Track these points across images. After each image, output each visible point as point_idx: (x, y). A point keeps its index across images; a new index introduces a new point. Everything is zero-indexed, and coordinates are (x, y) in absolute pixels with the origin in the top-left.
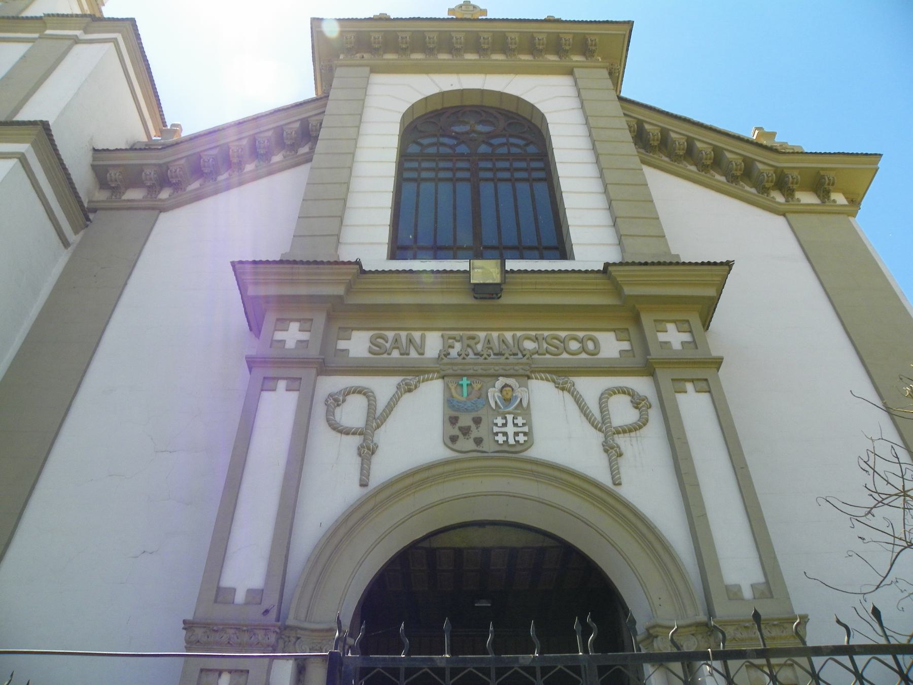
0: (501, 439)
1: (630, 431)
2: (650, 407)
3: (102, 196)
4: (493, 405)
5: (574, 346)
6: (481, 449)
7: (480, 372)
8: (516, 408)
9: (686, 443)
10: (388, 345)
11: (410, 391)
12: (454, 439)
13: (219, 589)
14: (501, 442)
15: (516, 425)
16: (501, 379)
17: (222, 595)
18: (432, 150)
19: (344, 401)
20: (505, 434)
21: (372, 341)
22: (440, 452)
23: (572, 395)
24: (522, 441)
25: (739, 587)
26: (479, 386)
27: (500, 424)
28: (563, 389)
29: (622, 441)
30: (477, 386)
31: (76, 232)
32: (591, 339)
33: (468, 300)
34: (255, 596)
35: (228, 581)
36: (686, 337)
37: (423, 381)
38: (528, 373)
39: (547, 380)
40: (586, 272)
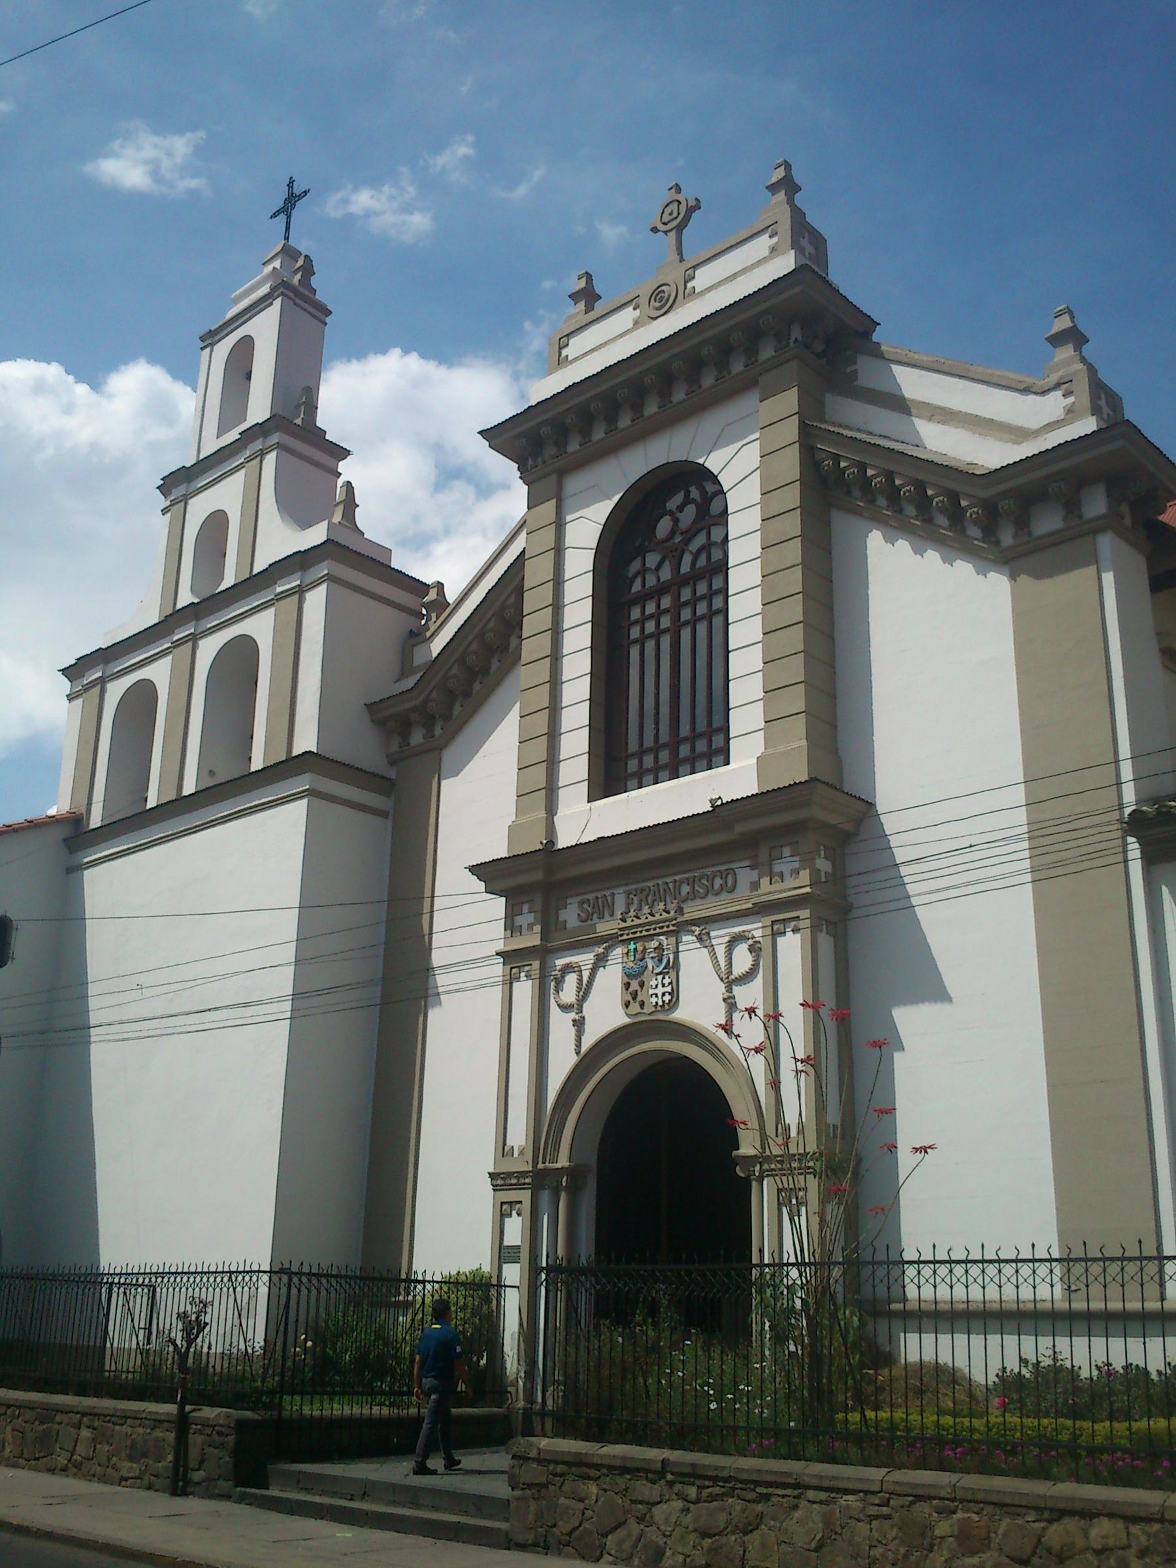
0: (654, 1000)
5: (718, 882)
6: (643, 1011)
7: (644, 933)
8: (664, 969)
10: (590, 909)
15: (663, 985)
16: (655, 937)
19: (563, 977)
20: (657, 995)
21: (582, 903)
22: (619, 1019)
26: (641, 948)
27: (654, 987)
29: (736, 990)
31: (388, 796)
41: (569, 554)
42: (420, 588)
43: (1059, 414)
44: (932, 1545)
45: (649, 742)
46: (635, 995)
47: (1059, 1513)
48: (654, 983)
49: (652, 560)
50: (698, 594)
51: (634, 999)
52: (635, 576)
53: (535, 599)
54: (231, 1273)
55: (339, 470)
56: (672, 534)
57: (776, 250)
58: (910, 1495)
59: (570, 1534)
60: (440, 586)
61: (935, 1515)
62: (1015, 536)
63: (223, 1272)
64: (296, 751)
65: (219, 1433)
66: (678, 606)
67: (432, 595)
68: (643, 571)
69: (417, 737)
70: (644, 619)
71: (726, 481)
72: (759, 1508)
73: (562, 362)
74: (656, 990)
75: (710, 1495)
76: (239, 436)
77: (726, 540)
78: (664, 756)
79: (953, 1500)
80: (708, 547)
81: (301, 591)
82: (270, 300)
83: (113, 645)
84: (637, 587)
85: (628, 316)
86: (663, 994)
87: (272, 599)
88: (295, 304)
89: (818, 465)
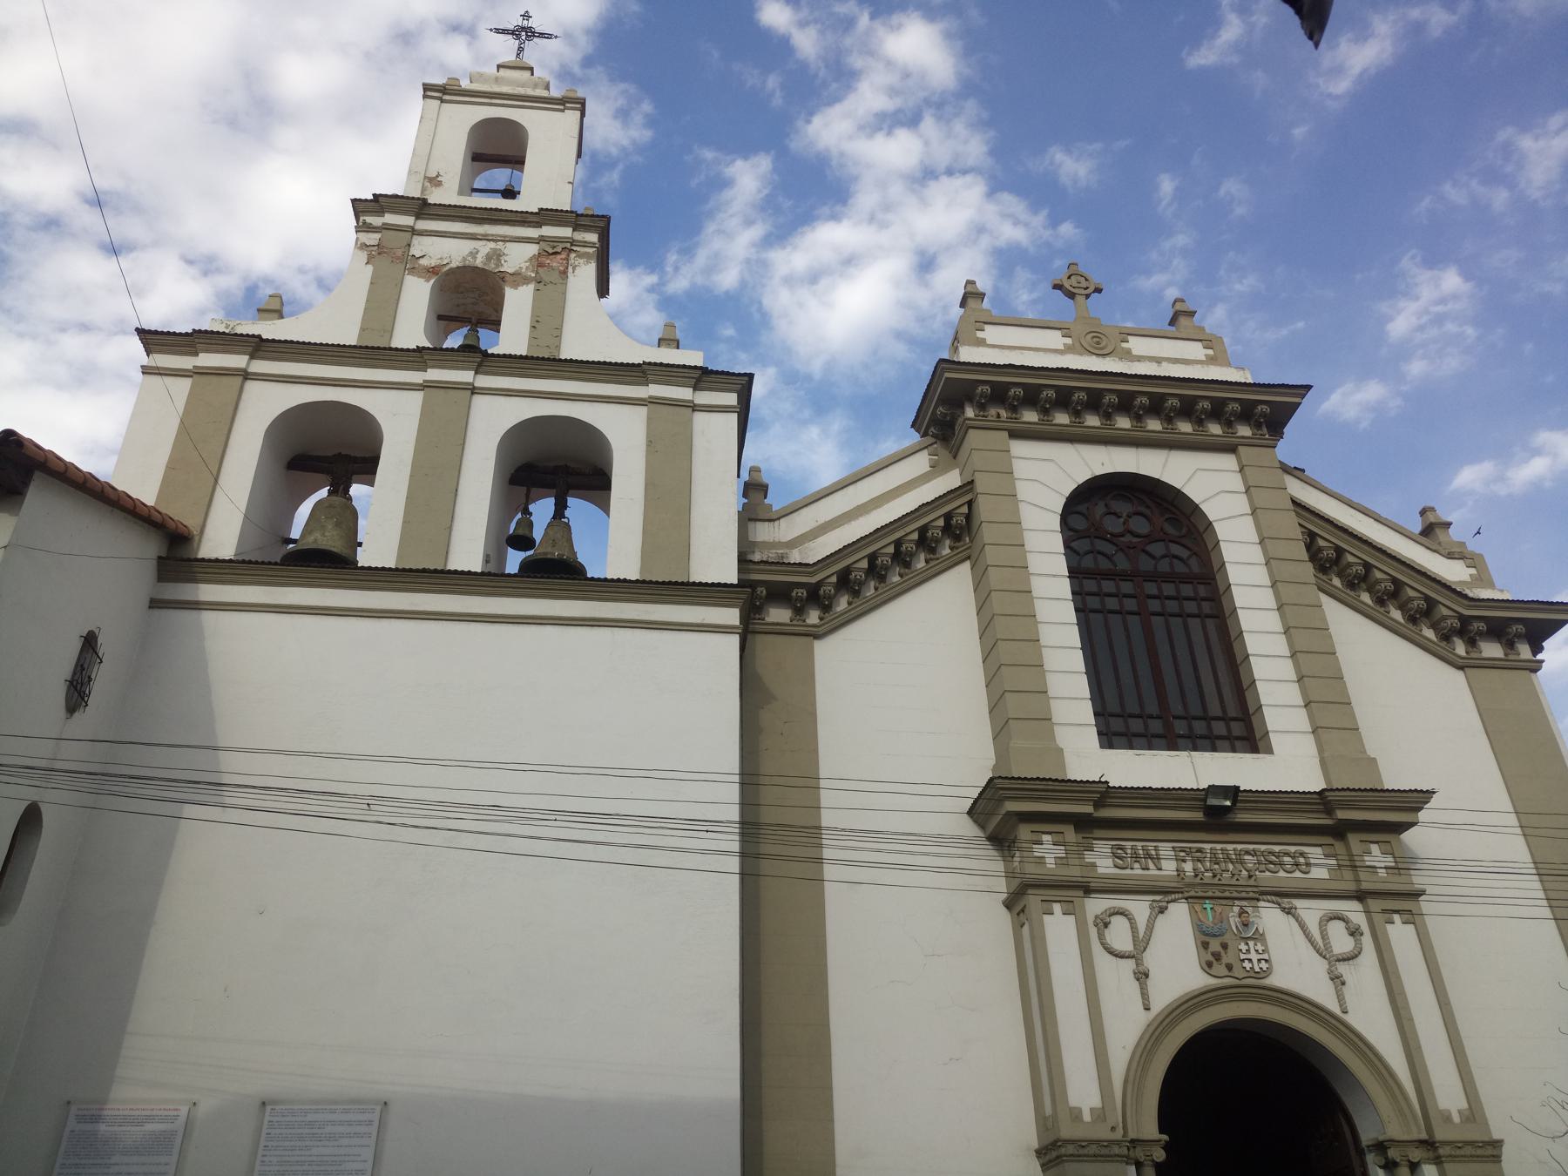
2: (1362, 934)
4: (1235, 931)
7: (1218, 894)
9: (1399, 977)
11: (1162, 912)
12: (1208, 966)
13: (1071, 1109)
14: (1248, 969)
15: (1257, 951)
16: (1237, 902)
17: (1076, 1114)
18: (1088, 562)
19: (1110, 923)
20: (1250, 960)
23: (1297, 920)
24: (1265, 969)
25: (1449, 1111)
26: (1220, 910)
27: (1244, 951)
28: (1288, 913)
29: (1342, 968)
30: (1219, 909)
32: (1302, 854)
34: (1100, 1115)
35: (1074, 1101)
36: (1389, 861)
38: (1257, 896)
39: (1273, 902)
40: (1304, 793)
46: (1217, 956)
57: (1216, 360)
69: (778, 615)
71: (1211, 510)
73: (982, 343)
81: (695, 408)
82: (562, 107)
83: (286, 341)
85: (1055, 339)
86: (1259, 960)
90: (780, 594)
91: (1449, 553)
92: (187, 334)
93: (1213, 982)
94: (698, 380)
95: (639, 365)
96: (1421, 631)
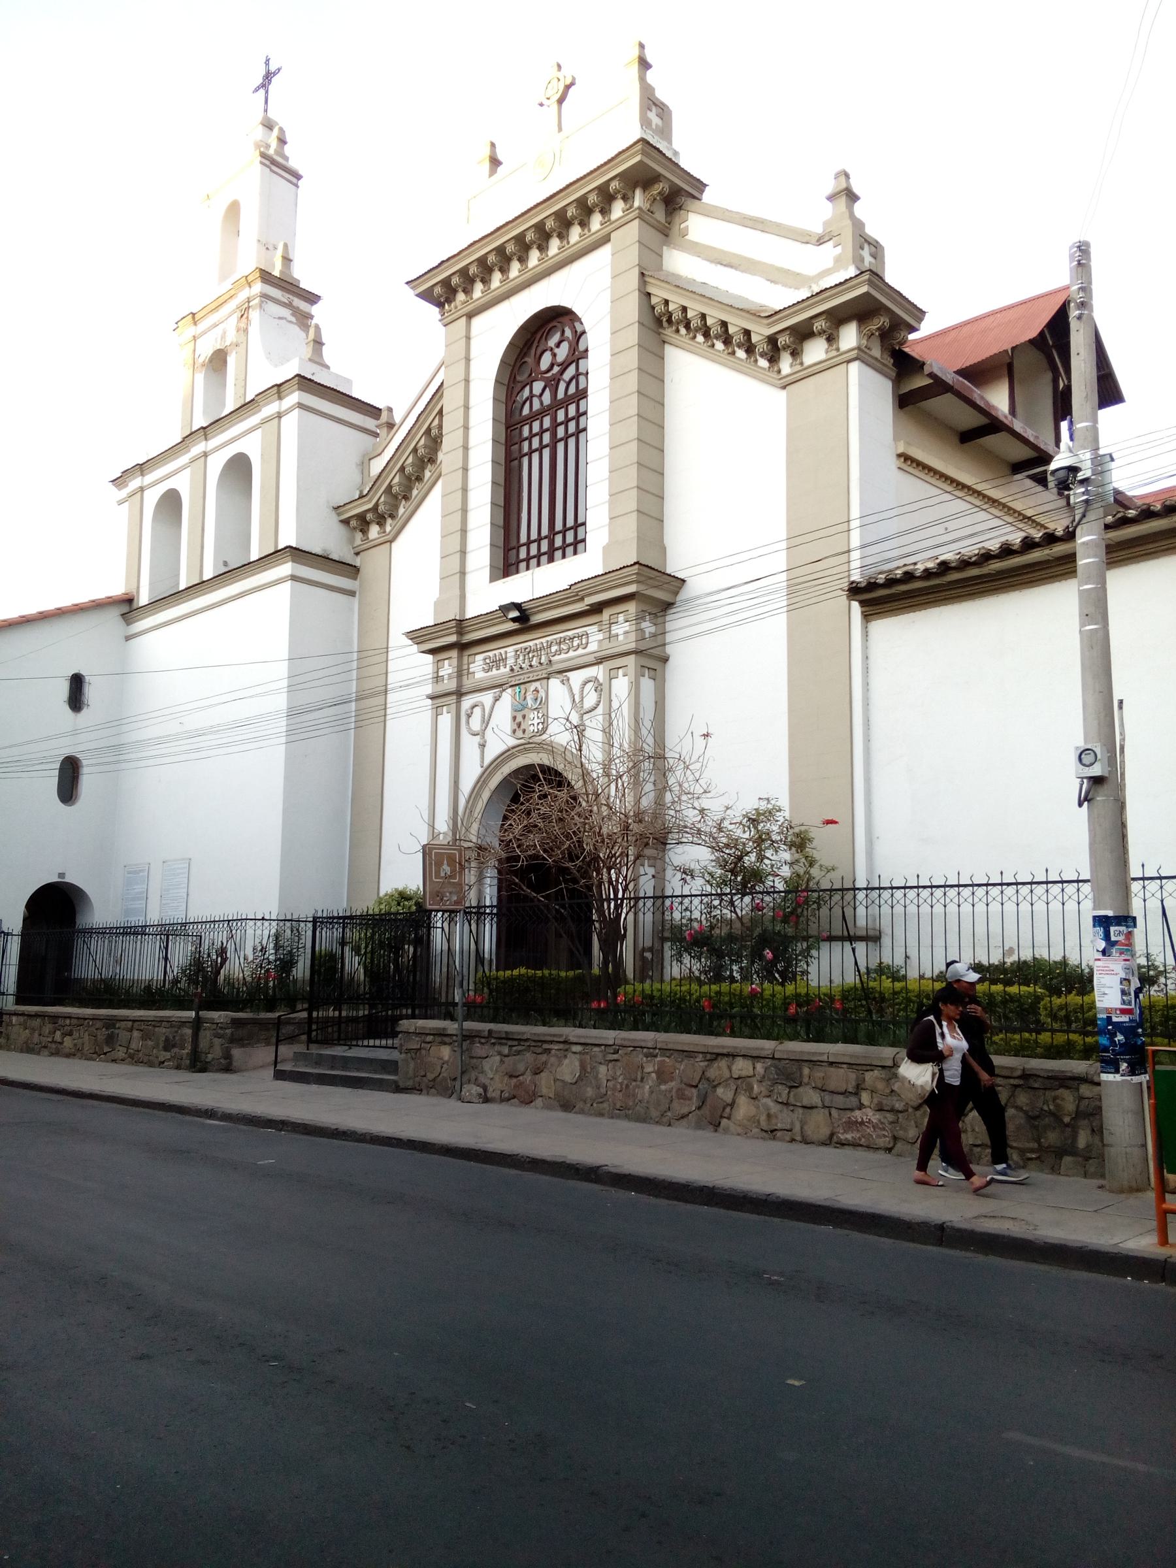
0: (532, 728)
1: (590, 711)
3: (359, 536)
4: (530, 706)
5: (576, 643)
7: (526, 680)
8: (540, 704)
11: (498, 700)
12: (514, 731)
15: (538, 717)
19: (472, 713)
22: (512, 742)
28: (564, 684)
31: (355, 579)
33: (515, 626)
37: (504, 690)
41: (472, 385)
42: (373, 411)
43: (830, 264)
44: (642, 1079)
45: (534, 536)
46: (519, 725)
47: (717, 1056)
48: (532, 716)
49: (538, 386)
50: (569, 416)
51: (519, 727)
52: (524, 403)
53: (451, 423)
54: (229, 921)
55: (313, 314)
56: (552, 366)
58: (630, 1047)
59: (434, 1080)
60: (390, 410)
61: (645, 1059)
62: (791, 366)
63: (224, 921)
64: (280, 547)
65: (221, 1028)
66: (555, 425)
67: (384, 417)
68: (531, 396)
69: (374, 531)
70: (532, 436)
72: (544, 1058)
74: (533, 722)
75: (516, 1051)
76: (232, 287)
77: (587, 373)
78: (545, 546)
79: (655, 1048)
80: (576, 377)
81: (279, 416)
84: (526, 411)
86: (538, 724)
87: (257, 425)
88: (271, 170)
89: (653, 308)
90: (363, 522)
91: (818, 241)
92: (121, 476)
93: (515, 742)
94: (279, 392)
95: (253, 400)
96: (756, 361)
